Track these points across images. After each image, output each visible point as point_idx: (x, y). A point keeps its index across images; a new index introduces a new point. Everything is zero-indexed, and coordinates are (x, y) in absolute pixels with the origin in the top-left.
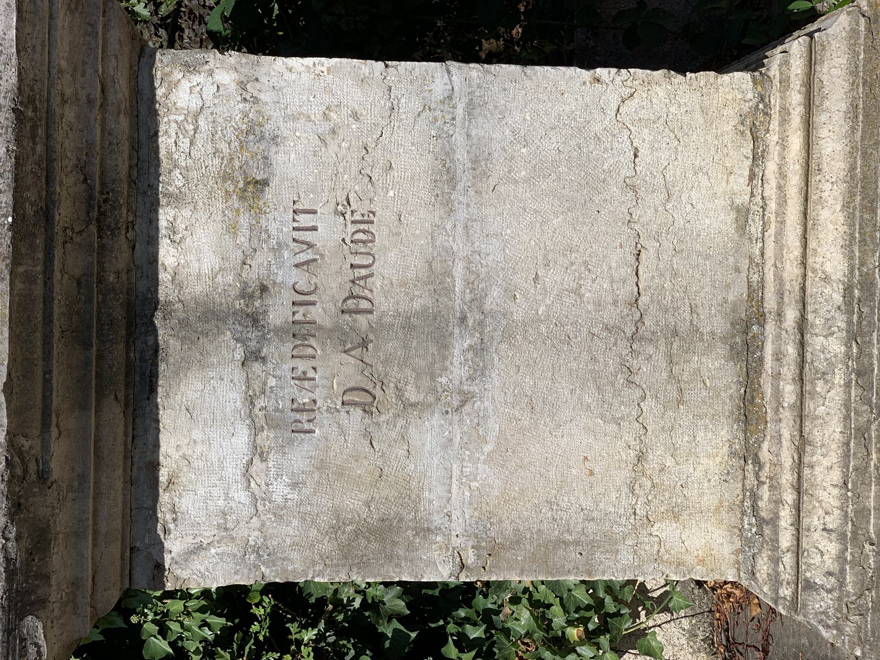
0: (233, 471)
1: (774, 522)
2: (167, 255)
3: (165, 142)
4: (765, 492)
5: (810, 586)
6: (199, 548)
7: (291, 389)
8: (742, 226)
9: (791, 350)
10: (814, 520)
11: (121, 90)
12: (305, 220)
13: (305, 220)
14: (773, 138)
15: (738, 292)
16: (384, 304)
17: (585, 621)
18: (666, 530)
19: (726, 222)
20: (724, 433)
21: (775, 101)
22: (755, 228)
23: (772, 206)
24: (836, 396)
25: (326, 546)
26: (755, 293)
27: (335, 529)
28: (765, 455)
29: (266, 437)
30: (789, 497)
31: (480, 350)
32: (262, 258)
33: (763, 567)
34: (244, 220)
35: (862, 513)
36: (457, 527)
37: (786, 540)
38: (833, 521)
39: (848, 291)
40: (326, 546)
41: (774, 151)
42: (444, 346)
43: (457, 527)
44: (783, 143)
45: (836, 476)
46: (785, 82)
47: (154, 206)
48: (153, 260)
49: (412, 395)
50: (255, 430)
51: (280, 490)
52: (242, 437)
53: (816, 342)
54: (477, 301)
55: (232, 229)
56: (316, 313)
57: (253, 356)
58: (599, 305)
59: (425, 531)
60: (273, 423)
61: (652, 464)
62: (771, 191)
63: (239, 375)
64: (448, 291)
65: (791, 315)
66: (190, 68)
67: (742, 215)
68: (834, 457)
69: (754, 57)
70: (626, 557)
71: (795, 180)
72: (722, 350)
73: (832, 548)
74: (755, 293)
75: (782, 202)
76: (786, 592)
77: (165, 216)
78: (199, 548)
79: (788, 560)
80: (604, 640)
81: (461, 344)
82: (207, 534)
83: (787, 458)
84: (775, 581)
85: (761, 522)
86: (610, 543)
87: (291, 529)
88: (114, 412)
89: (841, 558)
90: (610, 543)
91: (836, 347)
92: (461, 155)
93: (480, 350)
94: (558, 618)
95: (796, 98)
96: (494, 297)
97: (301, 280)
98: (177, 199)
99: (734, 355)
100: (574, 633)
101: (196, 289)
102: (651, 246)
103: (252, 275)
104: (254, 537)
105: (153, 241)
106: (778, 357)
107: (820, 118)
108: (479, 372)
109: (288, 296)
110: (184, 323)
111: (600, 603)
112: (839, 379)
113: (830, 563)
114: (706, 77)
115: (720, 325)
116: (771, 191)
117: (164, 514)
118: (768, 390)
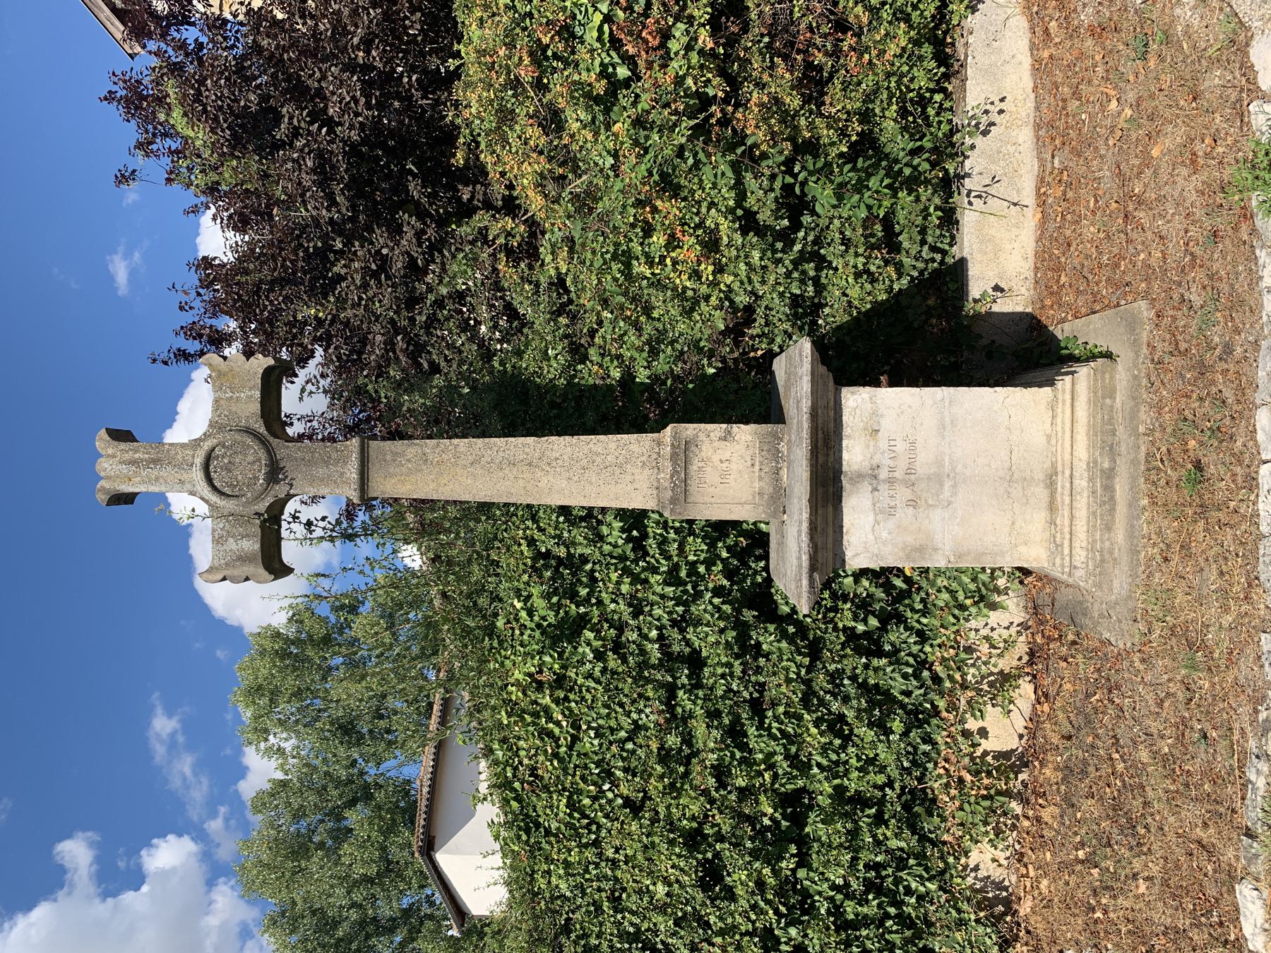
0: (868, 528)
1: (1062, 545)
2: (845, 456)
3: (844, 418)
4: (1058, 535)
5: (1075, 567)
6: (857, 555)
7: (888, 500)
8: (1049, 442)
9: (1068, 485)
10: (1076, 544)
11: (832, 404)
12: (892, 443)
13: (892, 443)
14: (1059, 410)
15: (1048, 464)
16: (920, 471)
17: (973, 597)
18: (1022, 549)
19: (1044, 439)
20: (1043, 515)
21: (1060, 397)
22: (1053, 442)
23: (1060, 434)
24: (1084, 501)
25: (901, 554)
26: (1054, 465)
27: (903, 549)
28: (1058, 522)
29: (880, 517)
30: (1068, 536)
31: (954, 486)
32: (878, 456)
33: (1058, 561)
34: (872, 443)
35: (1094, 541)
36: (947, 548)
37: (1066, 551)
38: (1084, 544)
39: (1088, 464)
40: (901, 554)
41: (1060, 415)
42: (941, 484)
43: (947, 548)
44: (1063, 412)
45: (1085, 528)
46: (1064, 391)
47: (841, 439)
48: (841, 458)
49: (930, 502)
50: (876, 515)
51: (885, 535)
52: (871, 517)
53: (1076, 482)
54: (953, 469)
55: (868, 446)
56: (896, 474)
57: (876, 489)
58: (997, 470)
59: (936, 550)
60: (882, 512)
61: (1017, 526)
62: (1059, 428)
63: (870, 496)
64: (943, 466)
65: (1067, 473)
66: (852, 393)
67: (1049, 437)
68: (1084, 522)
69: (1048, 373)
70: (1008, 559)
71: (1068, 425)
72: (1042, 485)
73: (1084, 553)
74: (1054, 465)
75: (1064, 433)
76: (1067, 570)
77: (844, 443)
78: (857, 555)
79: (1067, 558)
80: (982, 605)
81: (948, 484)
82: (860, 550)
83: (1067, 522)
84: (1063, 566)
85: (1057, 546)
86: (1002, 554)
87: (889, 548)
88: (830, 508)
89: (1087, 557)
90: (1002, 554)
91: (1084, 483)
92: (947, 420)
93: (954, 486)
94: (961, 596)
95: (1068, 397)
96: (959, 468)
97: (891, 463)
98: (849, 437)
99: (1047, 487)
100: (968, 602)
101: (855, 467)
102: (1016, 449)
103: (875, 462)
104: (876, 551)
105: (840, 451)
106: (1063, 487)
107: (1077, 404)
108: (954, 494)
109: (886, 469)
110: (851, 479)
111: (979, 590)
112: (1085, 494)
113: (1083, 559)
114: (1035, 389)
115: (1041, 476)
116: (1059, 428)
117: (845, 542)
118: (1059, 499)
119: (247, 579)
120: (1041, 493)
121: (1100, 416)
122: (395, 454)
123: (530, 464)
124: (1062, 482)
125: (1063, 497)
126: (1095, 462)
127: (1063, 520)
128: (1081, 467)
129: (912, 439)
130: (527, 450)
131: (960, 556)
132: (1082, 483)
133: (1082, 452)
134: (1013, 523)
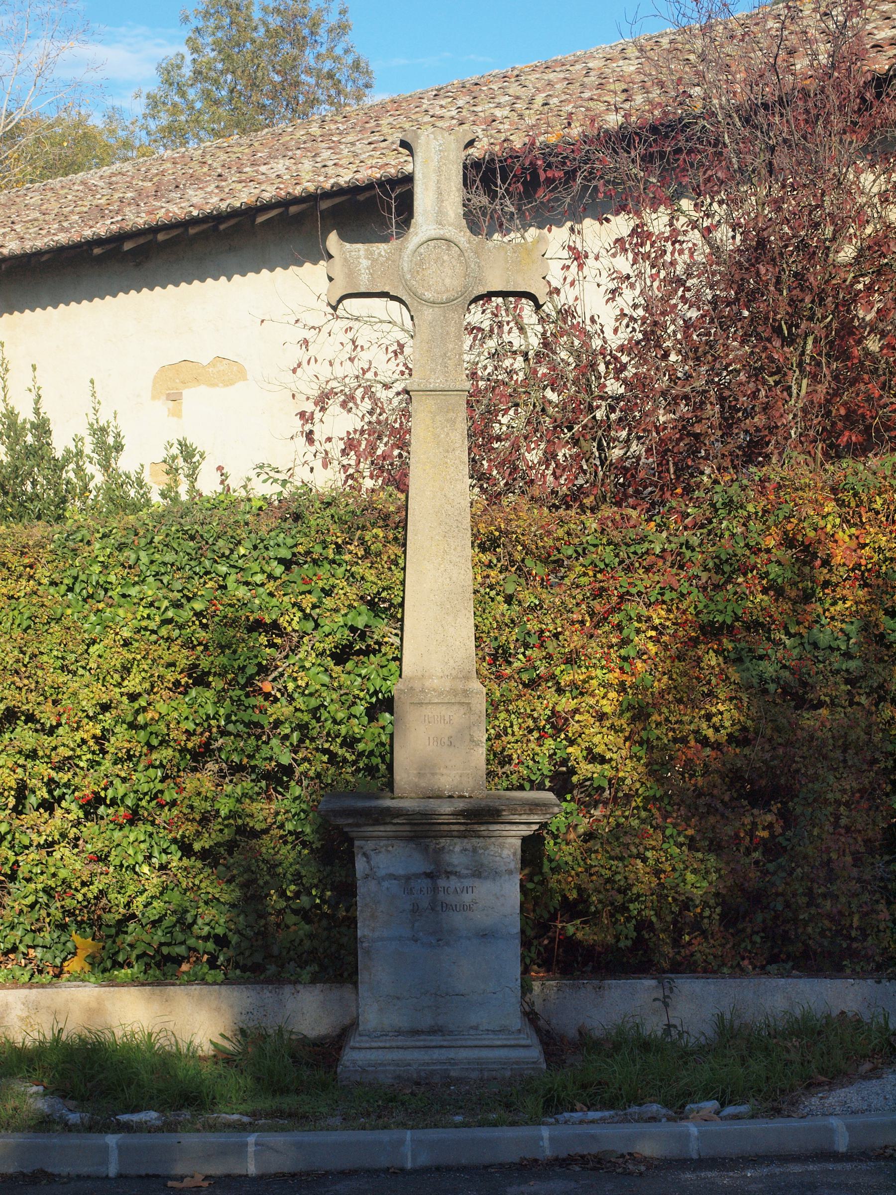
8: (471, 1028)
9: (434, 1044)
22: (472, 1032)
26: (451, 1033)
30: (388, 1045)
33: (364, 1038)
49: (417, 924)
53: (437, 1051)
56: (441, 894)
65: (445, 1044)
67: (476, 1028)
74: (451, 1033)
91: (435, 1056)
95: (512, 1042)
97: (451, 890)
119: (331, 279)
120: (427, 1021)
121: (495, 1066)
122: (453, 422)
123: (445, 552)
124: (437, 1040)
125: (421, 1041)
126: (456, 1064)
127: (401, 1041)
128: (452, 1054)
129: (474, 907)
130: (459, 549)
131: (367, 952)
132: (436, 1054)
133: (463, 1054)
134: (398, 998)
